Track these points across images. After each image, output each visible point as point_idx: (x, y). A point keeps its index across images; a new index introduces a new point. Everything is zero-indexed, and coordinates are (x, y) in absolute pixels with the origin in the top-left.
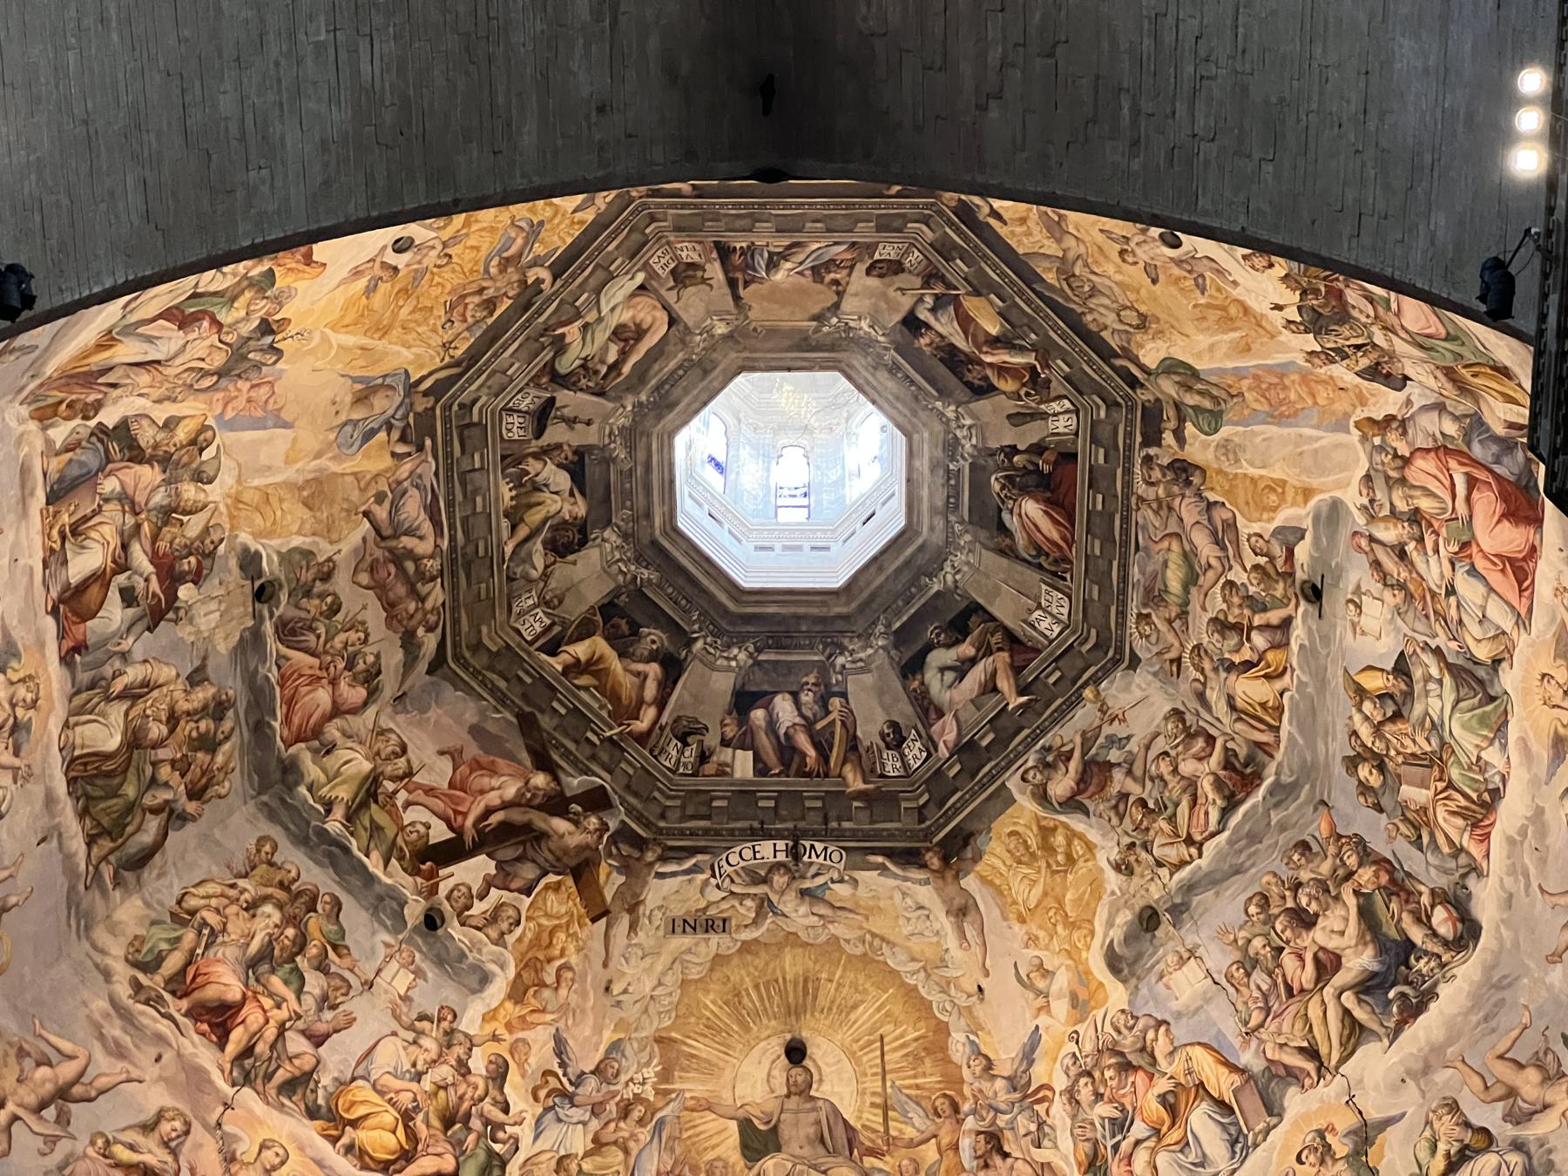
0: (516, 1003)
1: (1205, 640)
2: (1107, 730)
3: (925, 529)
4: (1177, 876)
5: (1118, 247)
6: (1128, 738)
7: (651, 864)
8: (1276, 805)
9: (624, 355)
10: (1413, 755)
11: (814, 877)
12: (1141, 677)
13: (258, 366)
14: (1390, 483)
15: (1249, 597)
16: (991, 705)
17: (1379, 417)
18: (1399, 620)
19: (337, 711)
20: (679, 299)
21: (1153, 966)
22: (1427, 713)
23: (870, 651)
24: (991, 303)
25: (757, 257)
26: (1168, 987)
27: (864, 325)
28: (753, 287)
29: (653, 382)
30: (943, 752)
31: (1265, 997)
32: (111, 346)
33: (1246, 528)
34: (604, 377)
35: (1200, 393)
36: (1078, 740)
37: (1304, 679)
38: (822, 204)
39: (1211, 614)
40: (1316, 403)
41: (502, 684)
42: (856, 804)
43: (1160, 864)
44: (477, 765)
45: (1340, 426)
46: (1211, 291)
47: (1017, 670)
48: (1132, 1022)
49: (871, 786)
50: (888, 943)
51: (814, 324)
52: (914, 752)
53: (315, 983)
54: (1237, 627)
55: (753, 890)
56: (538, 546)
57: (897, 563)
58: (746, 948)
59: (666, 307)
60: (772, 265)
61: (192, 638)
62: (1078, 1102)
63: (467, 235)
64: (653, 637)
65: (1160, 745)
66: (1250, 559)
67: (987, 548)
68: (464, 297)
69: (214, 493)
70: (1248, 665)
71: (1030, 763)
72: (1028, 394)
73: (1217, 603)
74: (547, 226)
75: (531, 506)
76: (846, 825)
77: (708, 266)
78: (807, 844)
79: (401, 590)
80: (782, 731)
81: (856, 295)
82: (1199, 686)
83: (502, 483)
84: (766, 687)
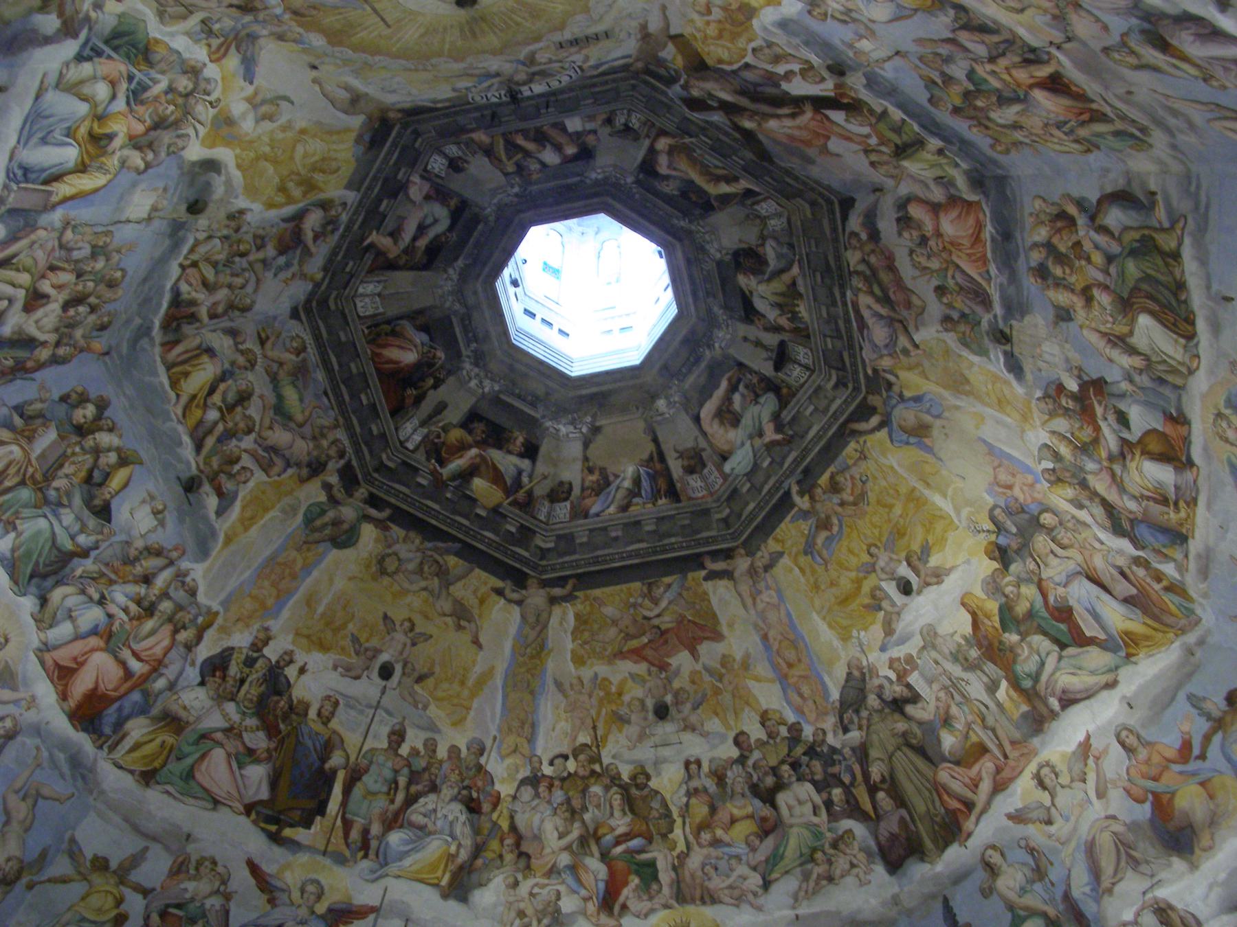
1: (250, 376)
3: (480, 289)
4: (191, 241)
5: (417, 630)
6: (275, 275)
7: (637, 60)
9: (728, 399)
10: (61, 466)
11: (490, 87)
12: (285, 306)
13: (1009, 512)
14: (179, 608)
16: (390, 224)
17: (209, 635)
18: (123, 537)
19: (935, 208)
20: (696, 438)
21: (176, 189)
22: (70, 506)
23: (495, 201)
24: (484, 507)
25: (649, 490)
26: (155, 190)
27: (563, 430)
28: (645, 456)
29: (703, 365)
30: (416, 179)
31: (70, 250)
32: (1127, 633)
33: (260, 475)
34: (739, 380)
35: (326, 524)
36: (313, 249)
37: (169, 424)
38: (613, 561)
39: (255, 398)
40: (250, 595)
41: (788, 180)
42: (474, 126)
43: (210, 237)
44: (808, 143)
45: (226, 603)
46: (347, 643)
47: (380, 253)
48: (172, 149)
50: (410, 70)
51: (598, 424)
52: (437, 164)
53: (958, 70)
54: (231, 408)
55: (542, 67)
56: (773, 263)
58: (538, 39)
59: (704, 434)
60: (637, 481)
61: (1067, 346)
62: (185, 72)
63: (858, 570)
64: (670, 188)
65: (250, 289)
66: (246, 461)
68: (855, 504)
69: (1044, 437)
70: (212, 391)
72: (439, 436)
73: (254, 410)
74: (801, 547)
75: (782, 294)
76: (477, 114)
78: (504, 98)
79: (885, 277)
81: (574, 460)
82: (239, 339)
84: (569, 165)
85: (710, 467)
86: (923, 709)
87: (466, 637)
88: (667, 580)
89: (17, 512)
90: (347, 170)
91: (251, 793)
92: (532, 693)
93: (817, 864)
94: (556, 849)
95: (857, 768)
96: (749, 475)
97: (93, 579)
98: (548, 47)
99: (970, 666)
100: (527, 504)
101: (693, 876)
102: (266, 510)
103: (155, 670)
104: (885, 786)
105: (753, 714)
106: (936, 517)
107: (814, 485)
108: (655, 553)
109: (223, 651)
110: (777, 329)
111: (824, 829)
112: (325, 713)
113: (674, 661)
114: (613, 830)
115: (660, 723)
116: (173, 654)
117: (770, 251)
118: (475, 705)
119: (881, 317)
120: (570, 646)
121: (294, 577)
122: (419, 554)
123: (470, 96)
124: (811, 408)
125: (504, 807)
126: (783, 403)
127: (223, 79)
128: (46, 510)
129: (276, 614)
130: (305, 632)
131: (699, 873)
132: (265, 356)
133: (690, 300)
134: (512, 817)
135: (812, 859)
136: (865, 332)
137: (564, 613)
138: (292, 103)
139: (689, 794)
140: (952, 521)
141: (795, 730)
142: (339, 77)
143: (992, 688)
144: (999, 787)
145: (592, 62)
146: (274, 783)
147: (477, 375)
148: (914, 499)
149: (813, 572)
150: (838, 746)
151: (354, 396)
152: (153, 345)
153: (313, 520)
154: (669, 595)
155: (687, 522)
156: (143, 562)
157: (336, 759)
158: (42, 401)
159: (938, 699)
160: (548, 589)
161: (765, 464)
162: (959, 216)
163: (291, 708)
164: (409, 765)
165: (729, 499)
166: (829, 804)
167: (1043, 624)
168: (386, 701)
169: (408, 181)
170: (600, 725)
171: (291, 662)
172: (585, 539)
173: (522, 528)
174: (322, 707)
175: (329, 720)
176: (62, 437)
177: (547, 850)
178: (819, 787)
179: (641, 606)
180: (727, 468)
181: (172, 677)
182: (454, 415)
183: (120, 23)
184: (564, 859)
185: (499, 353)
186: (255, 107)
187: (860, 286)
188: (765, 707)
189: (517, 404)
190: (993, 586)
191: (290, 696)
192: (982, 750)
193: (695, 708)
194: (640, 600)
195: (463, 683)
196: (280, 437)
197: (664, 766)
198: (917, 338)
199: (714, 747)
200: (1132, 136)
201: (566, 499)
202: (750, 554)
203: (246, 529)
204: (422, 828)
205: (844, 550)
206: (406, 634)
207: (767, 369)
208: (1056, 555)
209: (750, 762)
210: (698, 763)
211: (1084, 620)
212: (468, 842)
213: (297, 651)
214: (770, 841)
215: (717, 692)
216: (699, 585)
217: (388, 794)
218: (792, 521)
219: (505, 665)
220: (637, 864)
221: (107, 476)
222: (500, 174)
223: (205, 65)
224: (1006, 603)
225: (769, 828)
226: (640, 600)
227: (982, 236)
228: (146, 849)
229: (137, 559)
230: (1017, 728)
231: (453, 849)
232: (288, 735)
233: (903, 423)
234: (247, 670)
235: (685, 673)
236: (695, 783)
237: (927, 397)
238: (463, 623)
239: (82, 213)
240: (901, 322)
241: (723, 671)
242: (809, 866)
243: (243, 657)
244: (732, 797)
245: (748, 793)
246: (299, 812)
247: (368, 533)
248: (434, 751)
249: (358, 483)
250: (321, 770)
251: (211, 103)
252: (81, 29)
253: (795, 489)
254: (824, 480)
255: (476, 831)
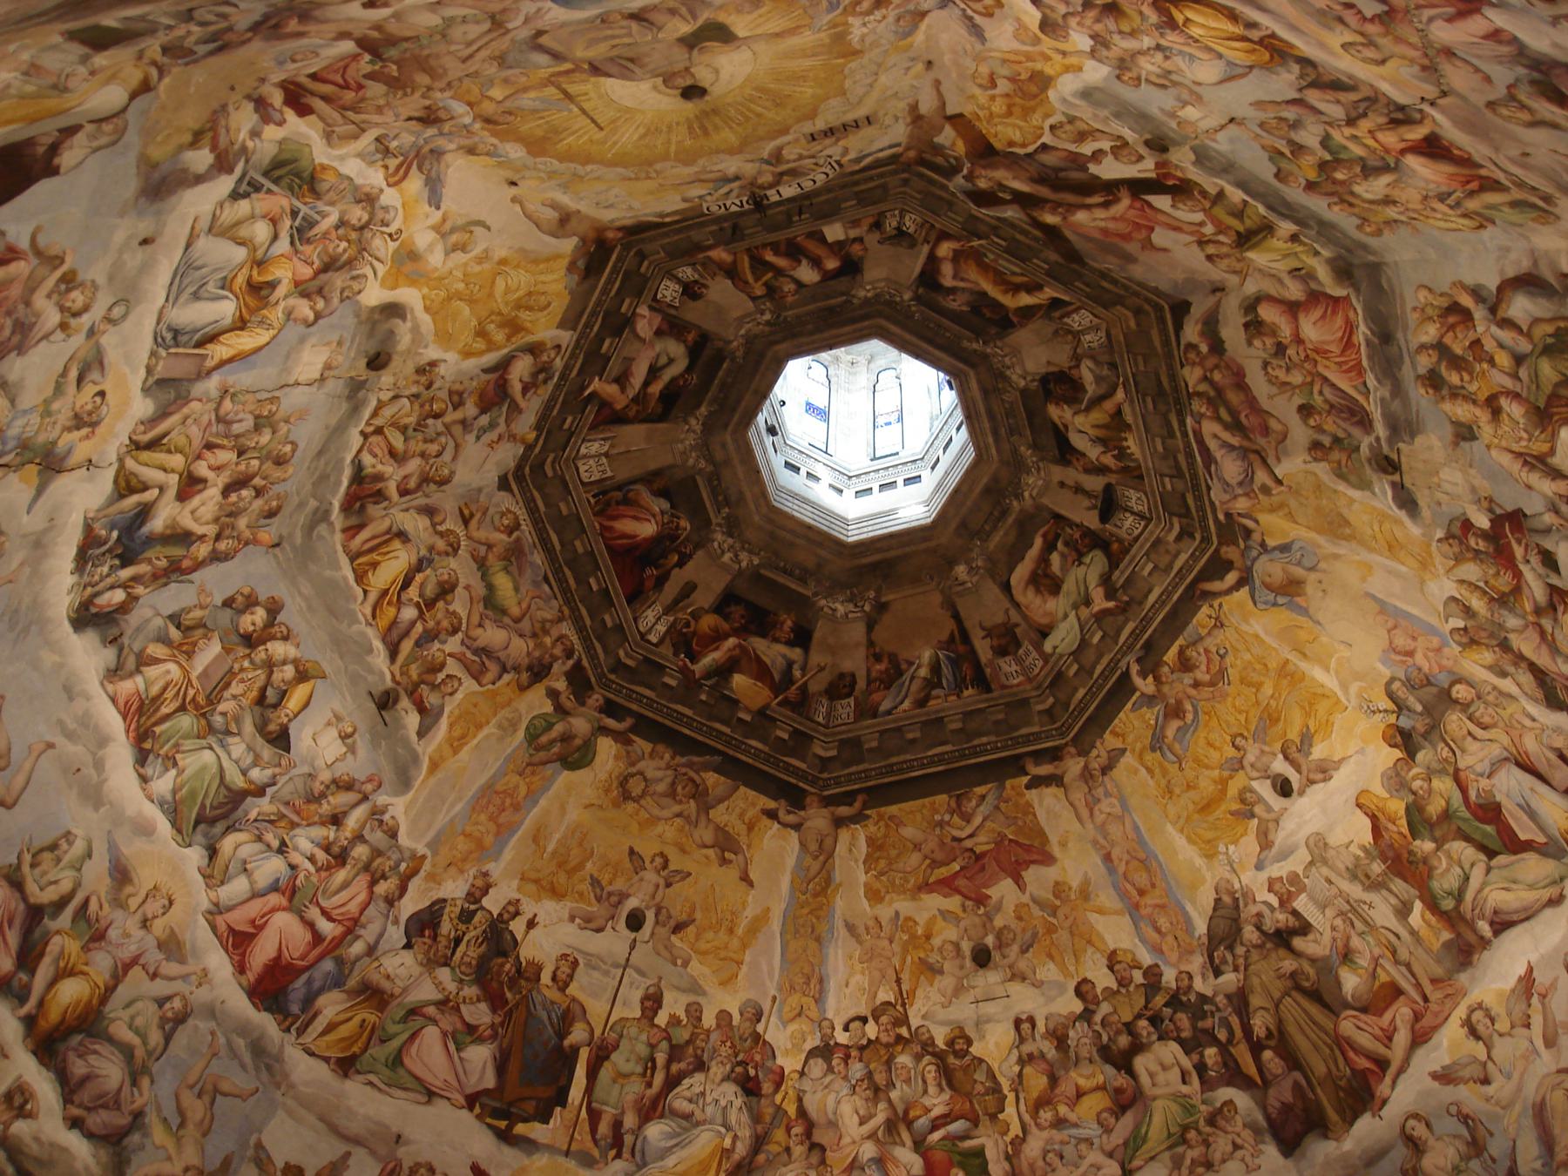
0: (1041, 73)
1: (453, 563)
2: (502, 428)
4: (374, 403)
5: (672, 867)
6: (478, 438)
7: (908, 149)
8: (317, 510)
9: (1044, 560)
10: (228, 685)
12: (491, 476)
13: (1410, 684)
14: (377, 853)
15: (436, 637)
16: (614, 367)
17: (414, 885)
18: (306, 769)
20: (1007, 611)
23: (743, 332)
24: (747, 710)
25: (951, 678)
26: (328, 344)
27: (841, 609)
28: (945, 636)
29: (1010, 520)
30: (643, 310)
31: (229, 423)
33: (469, 685)
34: (1057, 537)
35: (553, 741)
36: (522, 403)
37: (355, 627)
38: (912, 769)
39: (459, 590)
40: (464, 834)
41: (1105, 284)
43: (396, 397)
44: (1126, 237)
45: (434, 845)
46: (585, 887)
47: (604, 403)
49: (701, 256)
51: (884, 599)
52: (669, 291)
53: (1310, 136)
54: (430, 604)
56: (1091, 389)
57: (743, 404)
58: (785, 131)
59: (1017, 605)
60: (936, 668)
61: (1473, 472)
64: (956, 304)
65: (447, 456)
67: (671, 467)
68: (1212, 684)
69: (1450, 588)
70: (406, 584)
71: (558, 360)
72: (688, 625)
73: (459, 604)
76: (714, 228)
77: (990, 654)
79: (1234, 397)
80: (804, 262)
82: (438, 519)
83: (1138, 455)
84: (832, 283)
85: (1026, 645)
86: (1315, 941)
87: (732, 873)
88: (980, 790)
89: (177, 745)
90: (559, 305)
91: (474, 1079)
92: (818, 940)
93: (1190, 1147)
94: (857, 1138)
95: (1235, 1021)
96: (1077, 654)
97: (271, 822)
98: (797, 140)
99: (1374, 885)
100: (801, 704)
101: (1032, 1166)
102: (479, 727)
103: (349, 931)
104: (1272, 1043)
105: (1098, 955)
106: (1316, 698)
107: (1159, 663)
108: (963, 757)
109: (433, 904)
110: (1102, 470)
111: (1197, 1100)
112: (562, 976)
113: (994, 892)
114: (928, 1111)
115: (981, 972)
116: (371, 911)
117: (1087, 374)
118: (747, 958)
119: (1232, 448)
120: (862, 878)
121: (516, 807)
122: (670, 772)
123: (705, 206)
124: (1150, 566)
125: (789, 1086)
126: (1114, 562)
127: (404, 205)
128: (212, 740)
129: (496, 857)
130: (534, 875)
131: (1040, 1163)
132: (469, 538)
133: (990, 440)
134: (800, 1100)
135: (1184, 1141)
136: (1213, 468)
137: (853, 837)
138: (489, 229)
139: (1022, 1062)
140: (1338, 701)
141: (1153, 974)
142: (543, 193)
143: (1403, 911)
144: (1419, 1039)
145: (852, 155)
146: (501, 1068)
147: (731, 547)
148: (1286, 673)
149: (1165, 772)
150: (1209, 993)
151: (582, 580)
152: (333, 532)
153: (539, 736)
154: (984, 809)
155: (1001, 716)
156: (331, 798)
157: (577, 1034)
158: (202, 607)
159: (1333, 929)
160: (832, 809)
161: (1096, 640)
162: (1323, 317)
163: (519, 971)
164: (669, 1038)
165: (1052, 685)
166: (1201, 1068)
167: (1461, 824)
168: (639, 957)
169: (634, 313)
170: (905, 976)
171: (517, 913)
172: (874, 744)
173: (796, 733)
174: (557, 968)
175: (567, 985)
176: (227, 650)
177: (846, 1140)
178: (1188, 1046)
179: (948, 823)
180: (1048, 646)
181: (371, 940)
182: (704, 598)
183: (281, 151)
184: (868, 1151)
185: (756, 518)
186: (443, 236)
187: (1203, 410)
188: (1112, 947)
189: (782, 579)
190: (1396, 780)
191: (518, 957)
192: (1395, 992)
193: (1024, 951)
194: (947, 817)
195: (731, 931)
196: (493, 635)
197: (988, 1026)
198: (1279, 472)
199: (1050, 1000)
200: (1534, 206)
201: (849, 695)
202: (1083, 753)
203: (456, 751)
204: (687, 1117)
205: (1202, 742)
206: (658, 872)
207: (1092, 520)
208: (1475, 738)
209: (1098, 1018)
210: (1032, 1021)
211: (1516, 819)
212: (745, 1133)
213: (524, 900)
214: (1128, 1119)
215: (1051, 930)
216: (1022, 795)
217: (644, 1075)
218: (1133, 709)
219: (783, 906)
220: (960, 1154)
221: (283, 694)
222: (746, 298)
223: (382, 191)
224: (1415, 802)
225: (1126, 1101)
226: (947, 817)
227: (1354, 339)
228: (348, 1154)
229: (323, 795)
230: (1438, 961)
231: (727, 1142)
232: (517, 1005)
233: (1268, 580)
234: (462, 927)
235: (1009, 907)
236: (1028, 1048)
237: (1295, 547)
238: (727, 855)
239: (242, 378)
240: (1257, 452)
241: (1058, 903)
242: (1180, 1149)
243: (458, 910)
244: (1076, 1064)
245: (1096, 1057)
246: (534, 1103)
247: (606, 748)
248: (700, 1019)
249: (591, 688)
250: (559, 1048)
251: (390, 235)
252: (235, 164)
253: (1135, 668)
254: (1171, 655)
255: (756, 1118)
